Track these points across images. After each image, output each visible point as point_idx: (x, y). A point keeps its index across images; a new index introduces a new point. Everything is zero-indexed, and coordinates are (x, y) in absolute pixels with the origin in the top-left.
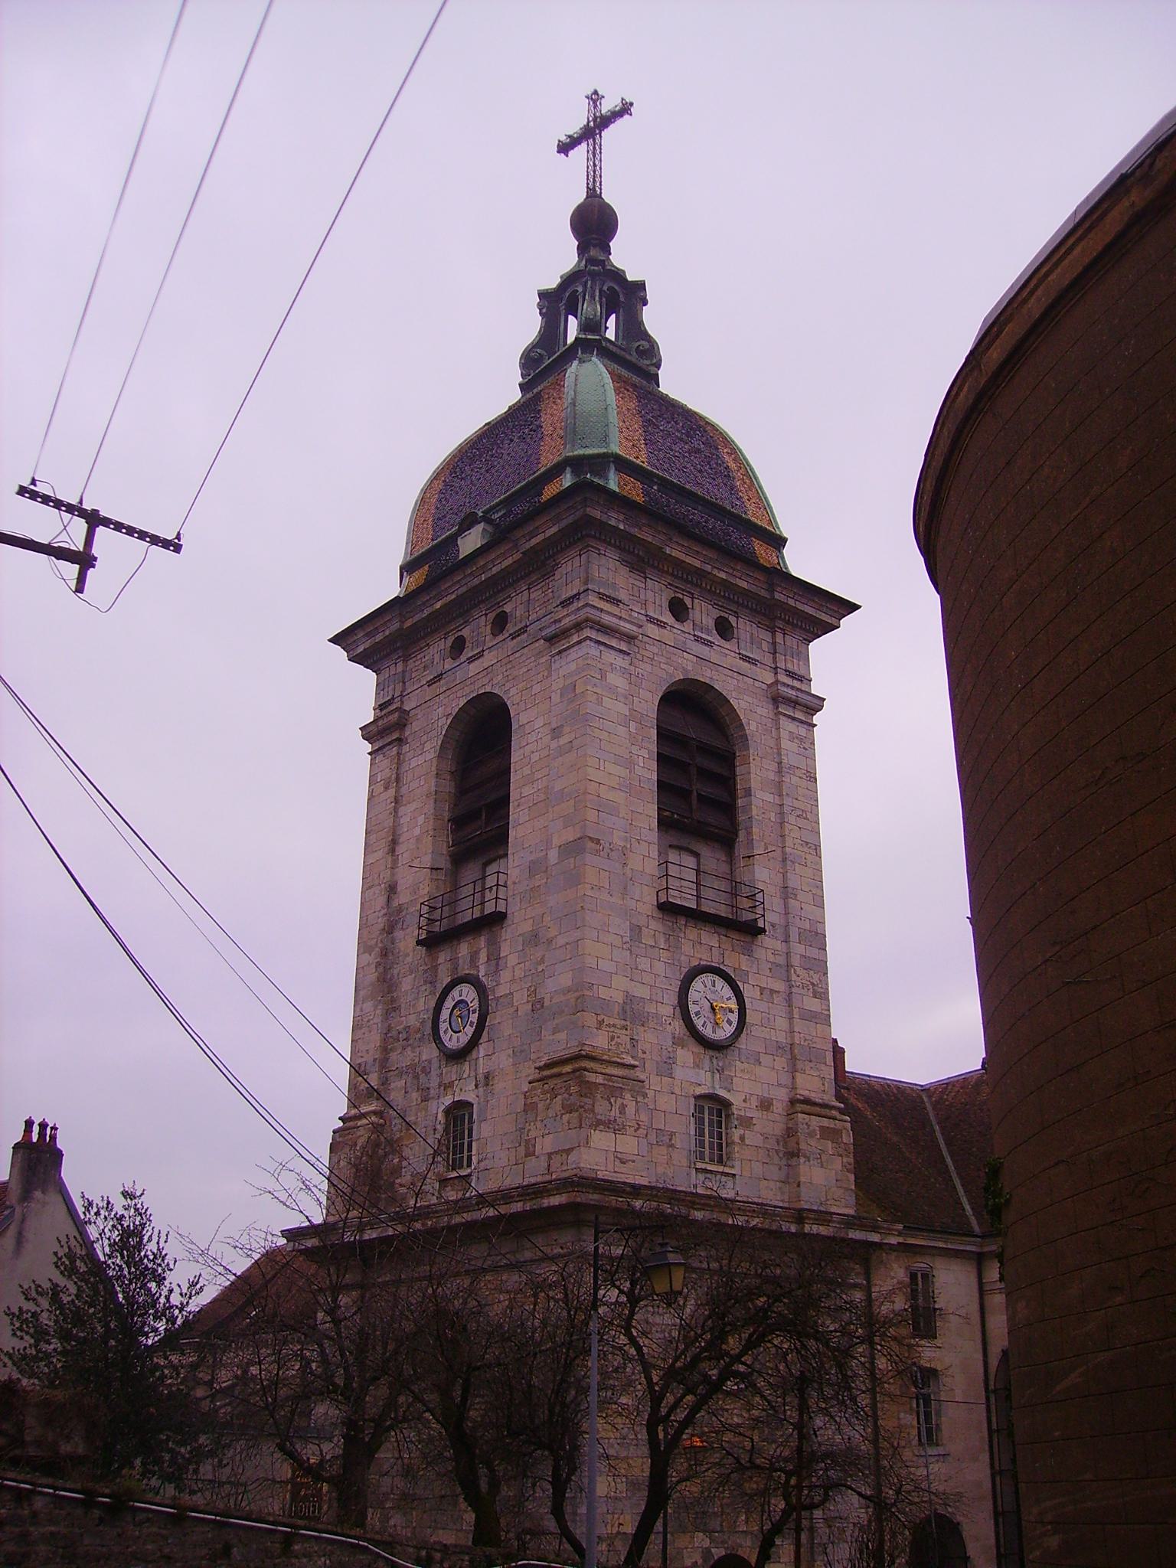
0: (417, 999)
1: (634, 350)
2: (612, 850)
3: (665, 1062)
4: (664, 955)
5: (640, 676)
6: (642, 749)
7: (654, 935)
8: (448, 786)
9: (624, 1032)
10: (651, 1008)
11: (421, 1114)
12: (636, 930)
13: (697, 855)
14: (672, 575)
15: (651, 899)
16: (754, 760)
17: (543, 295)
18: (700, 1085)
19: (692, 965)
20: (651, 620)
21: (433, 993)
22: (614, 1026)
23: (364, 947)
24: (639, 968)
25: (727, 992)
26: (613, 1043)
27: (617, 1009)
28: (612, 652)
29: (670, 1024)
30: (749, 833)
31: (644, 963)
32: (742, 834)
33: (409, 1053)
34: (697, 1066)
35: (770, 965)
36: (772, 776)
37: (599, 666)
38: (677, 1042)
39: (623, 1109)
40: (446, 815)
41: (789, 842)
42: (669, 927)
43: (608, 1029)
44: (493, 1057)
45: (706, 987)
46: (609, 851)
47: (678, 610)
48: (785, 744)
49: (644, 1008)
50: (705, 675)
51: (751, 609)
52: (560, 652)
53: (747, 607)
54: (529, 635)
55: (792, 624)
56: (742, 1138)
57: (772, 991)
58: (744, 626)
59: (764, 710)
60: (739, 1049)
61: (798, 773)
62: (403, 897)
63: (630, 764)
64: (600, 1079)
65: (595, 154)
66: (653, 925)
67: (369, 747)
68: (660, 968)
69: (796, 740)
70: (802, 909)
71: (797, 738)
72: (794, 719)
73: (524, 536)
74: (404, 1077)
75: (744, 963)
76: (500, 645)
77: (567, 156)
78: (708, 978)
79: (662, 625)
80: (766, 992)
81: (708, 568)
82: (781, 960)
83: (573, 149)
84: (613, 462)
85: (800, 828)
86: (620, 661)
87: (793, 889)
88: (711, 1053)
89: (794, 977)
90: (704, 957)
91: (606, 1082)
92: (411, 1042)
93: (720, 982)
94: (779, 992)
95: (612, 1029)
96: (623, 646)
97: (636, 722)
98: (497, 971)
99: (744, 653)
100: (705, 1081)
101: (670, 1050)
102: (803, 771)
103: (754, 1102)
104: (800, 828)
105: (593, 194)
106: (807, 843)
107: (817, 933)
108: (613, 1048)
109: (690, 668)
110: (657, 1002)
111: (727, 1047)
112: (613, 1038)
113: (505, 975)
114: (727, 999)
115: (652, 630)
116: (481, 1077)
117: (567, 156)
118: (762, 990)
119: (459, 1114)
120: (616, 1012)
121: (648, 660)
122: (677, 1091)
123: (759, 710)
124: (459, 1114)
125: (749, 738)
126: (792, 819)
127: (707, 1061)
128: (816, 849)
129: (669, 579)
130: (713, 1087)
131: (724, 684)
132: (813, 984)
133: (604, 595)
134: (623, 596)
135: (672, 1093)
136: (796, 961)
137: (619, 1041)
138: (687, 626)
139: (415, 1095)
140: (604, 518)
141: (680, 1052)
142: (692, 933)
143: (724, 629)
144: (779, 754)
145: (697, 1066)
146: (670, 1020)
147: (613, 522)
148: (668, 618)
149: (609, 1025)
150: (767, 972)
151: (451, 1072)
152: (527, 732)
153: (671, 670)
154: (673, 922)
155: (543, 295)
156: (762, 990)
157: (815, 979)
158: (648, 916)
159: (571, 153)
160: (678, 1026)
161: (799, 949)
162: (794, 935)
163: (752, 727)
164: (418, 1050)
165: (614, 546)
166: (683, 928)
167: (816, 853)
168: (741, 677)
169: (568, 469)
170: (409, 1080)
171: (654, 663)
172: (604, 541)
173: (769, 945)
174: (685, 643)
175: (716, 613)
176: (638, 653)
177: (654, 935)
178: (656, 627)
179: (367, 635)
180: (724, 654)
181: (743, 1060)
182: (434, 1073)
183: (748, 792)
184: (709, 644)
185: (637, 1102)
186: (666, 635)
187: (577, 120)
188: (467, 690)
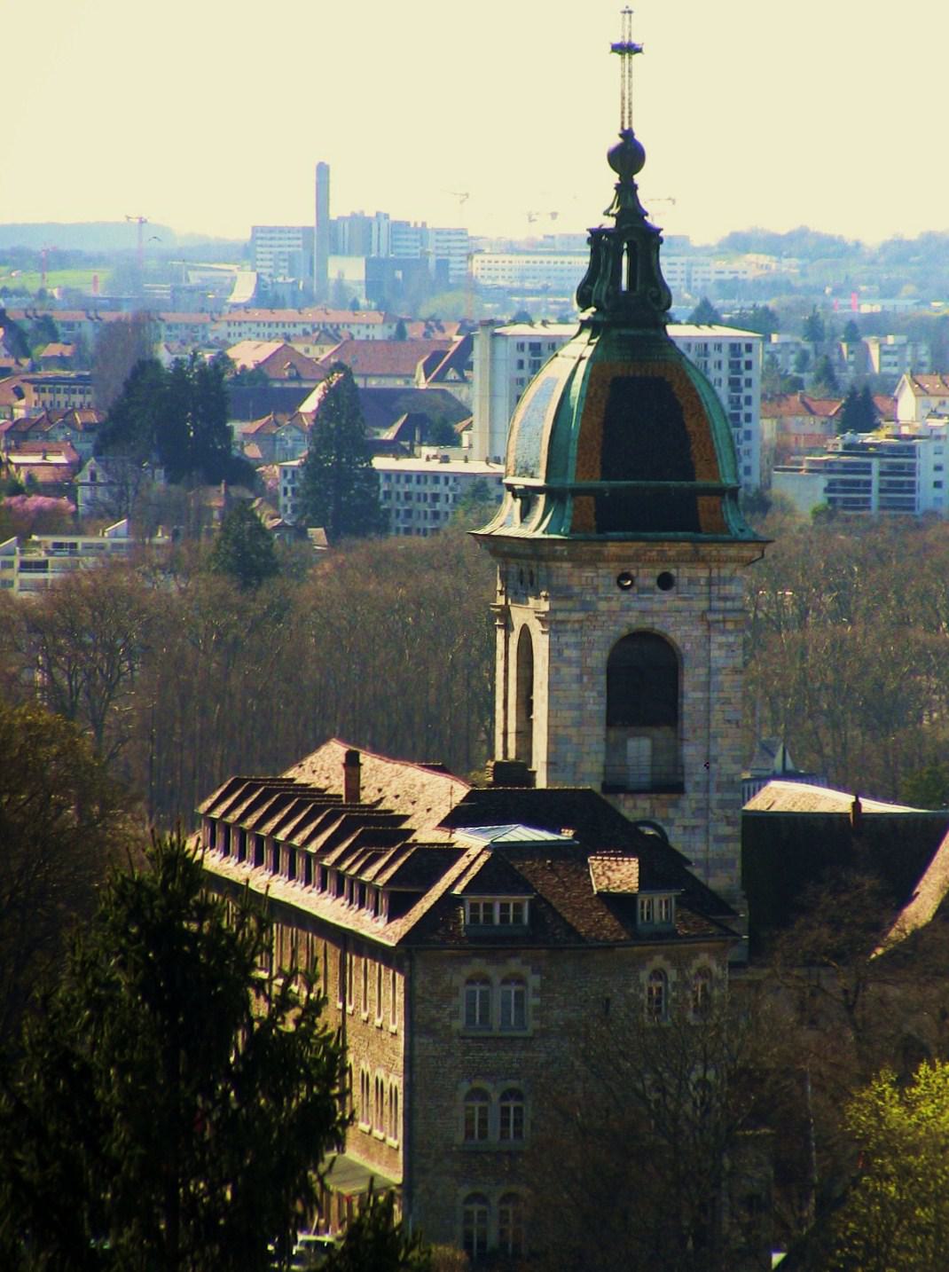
41: (713, 724)
48: (715, 653)
50: (646, 623)
61: (724, 672)
75: (671, 813)
82: (703, 805)
89: (711, 815)
105: (627, 135)
118: (685, 828)
123: (695, 633)
132: (727, 817)
136: (713, 804)
143: (666, 582)
144: (709, 661)
162: (713, 786)
173: (691, 799)
180: (668, 599)
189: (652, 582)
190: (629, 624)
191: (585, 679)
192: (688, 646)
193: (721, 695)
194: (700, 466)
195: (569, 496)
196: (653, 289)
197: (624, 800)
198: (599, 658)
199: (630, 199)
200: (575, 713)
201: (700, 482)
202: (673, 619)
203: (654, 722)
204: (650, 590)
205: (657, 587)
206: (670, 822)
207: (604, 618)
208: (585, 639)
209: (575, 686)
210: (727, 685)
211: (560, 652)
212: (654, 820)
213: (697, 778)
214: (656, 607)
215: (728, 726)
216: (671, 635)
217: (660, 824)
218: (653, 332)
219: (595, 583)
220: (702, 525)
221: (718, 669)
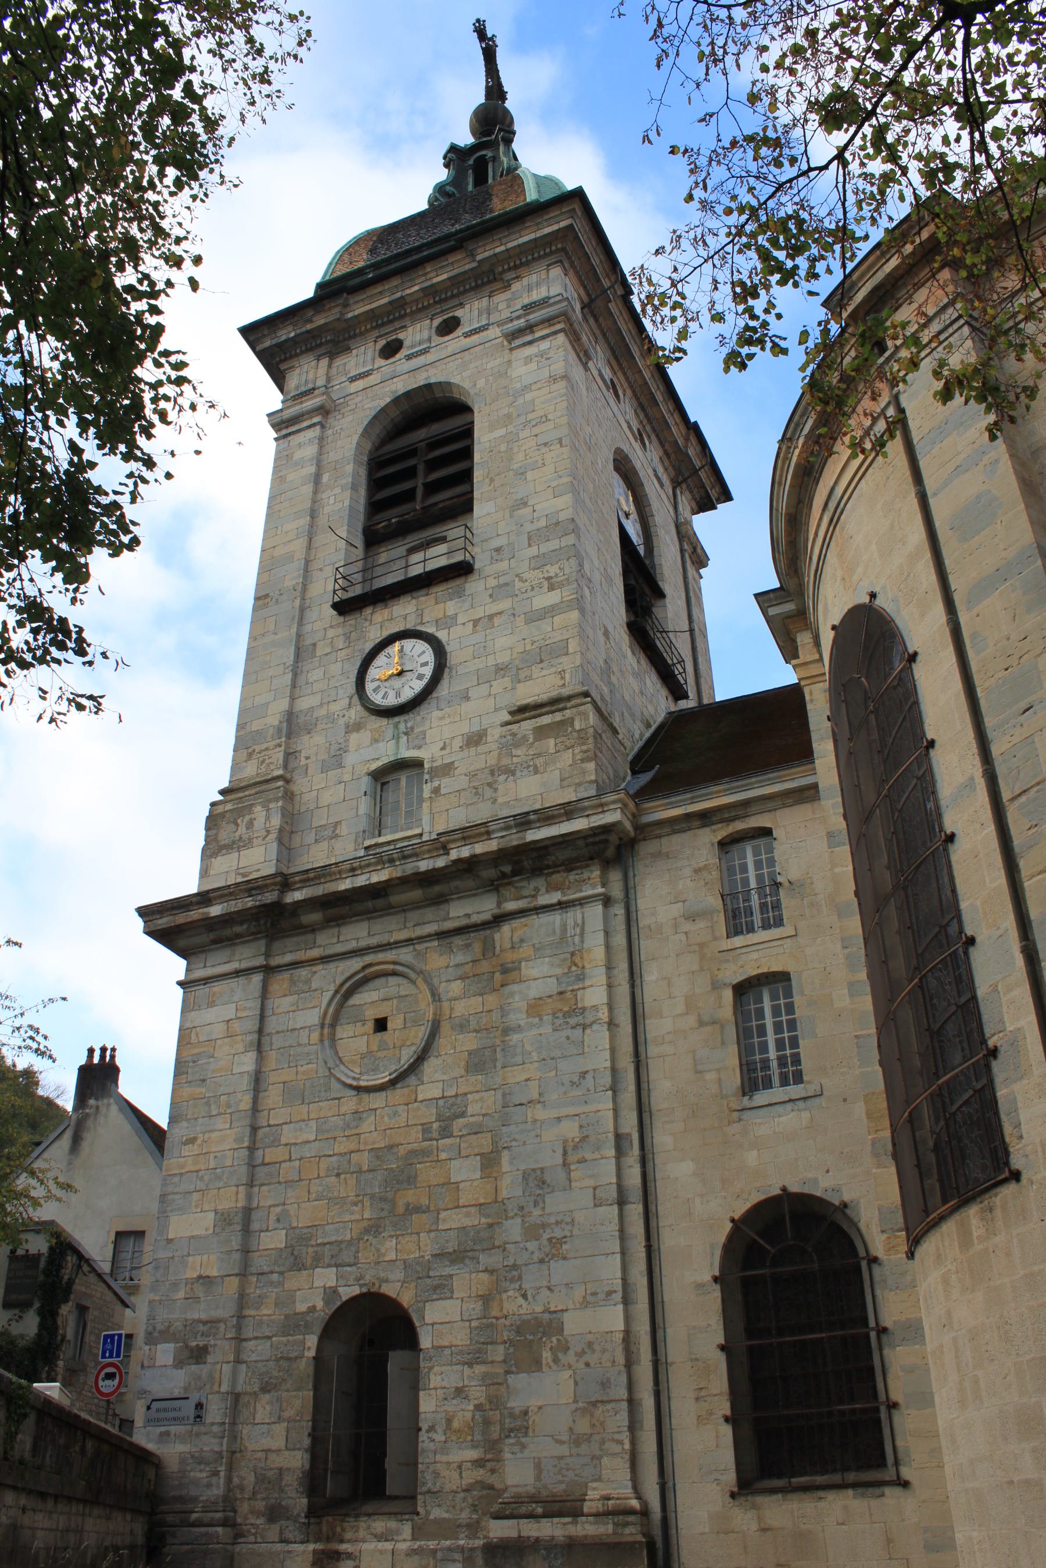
14: (373, 328)
22: (267, 749)
35: (490, 591)
39: (250, 825)
50: (420, 380)
51: (472, 289)
53: (466, 291)
55: (522, 265)
56: (436, 791)
57: (491, 617)
81: (398, 295)
88: (396, 719)
100: (386, 752)
103: (458, 743)
112: (263, 762)
118: (476, 622)
129: (376, 333)
140: (274, 342)
141: (354, 737)
143: (449, 327)
147: (284, 338)
160: (357, 712)
165: (302, 352)
172: (291, 357)
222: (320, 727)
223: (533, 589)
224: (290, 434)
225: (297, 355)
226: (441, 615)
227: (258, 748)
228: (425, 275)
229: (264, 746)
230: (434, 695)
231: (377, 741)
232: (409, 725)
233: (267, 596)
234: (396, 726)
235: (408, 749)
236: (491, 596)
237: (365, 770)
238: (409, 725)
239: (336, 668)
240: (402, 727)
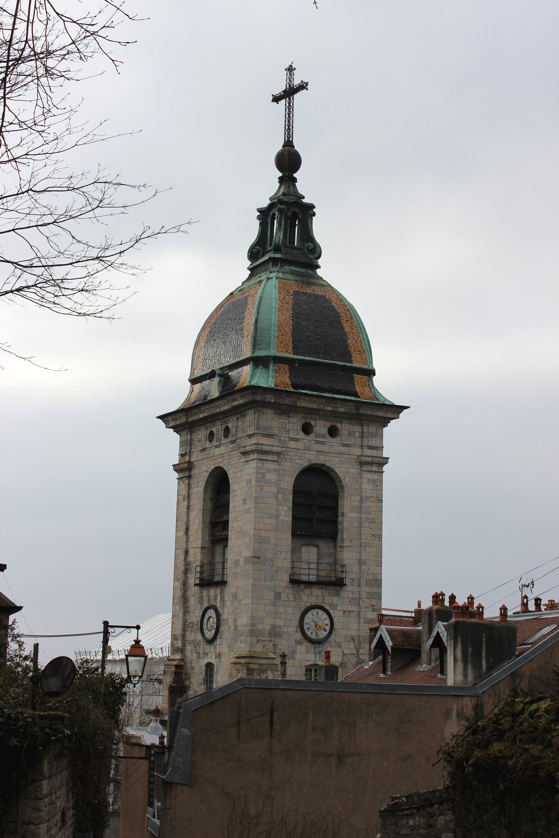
0: (196, 609)
1: (306, 248)
2: (266, 560)
3: (291, 653)
4: (292, 604)
5: (284, 470)
6: (284, 507)
7: (288, 595)
8: (209, 506)
9: (270, 643)
10: (285, 629)
11: (197, 664)
12: (278, 596)
13: (317, 547)
15: (286, 578)
16: (347, 497)
17: (260, 210)
18: (308, 661)
19: (307, 606)
20: (291, 439)
21: (201, 609)
22: (265, 641)
23: (176, 579)
24: (279, 612)
25: (325, 616)
26: (264, 649)
27: (267, 633)
28: (269, 462)
29: (294, 635)
30: (342, 535)
31: (281, 610)
32: (339, 535)
33: (193, 634)
34: (307, 652)
35: (349, 599)
36: (357, 504)
37: (262, 471)
38: (298, 643)
40: (208, 520)
41: (364, 536)
42: (295, 590)
43: (262, 643)
44: (222, 646)
45: (313, 616)
46: (265, 561)
47: (307, 429)
48: (365, 486)
49: (281, 630)
50: (321, 460)
51: (348, 418)
52: (246, 461)
54: (237, 445)
57: (350, 612)
58: (344, 428)
59: (354, 470)
60: (330, 641)
61: (371, 499)
62: (191, 558)
63: (277, 517)
64: (256, 667)
65: (290, 109)
66: (287, 590)
67: (176, 475)
68: (290, 610)
69: (372, 483)
70: (369, 569)
71: (372, 481)
72: (370, 471)
73: (231, 399)
74: (191, 645)
75: (335, 600)
76: (226, 444)
77: (278, 104)
78: (314, 612)
79: (296, 440)
80: (347, 613)
82: (356, 596)
83: (280, 100)
84: (272, 359)
85: (370, 528)
86: (273, 466)
87: (364, 560)
88: (315, 645)
89: (362, 603)
90: (313, 601)
91: (259, 667)
92: (193, 629)
93: (321, 612)
94: (353, 612)
95: (264, 642)
96: (275, 458)
97: (282, 494)
98: (223, 607)
99: (344, 442)
101: (294, 647)
102: (375, 498)
104: (370, 528)
105: (289, 143)
106: (374, 535)
107: (376, 580)
108: (265, 650)
109: (312, 458)
110: (288, 626)
111: (323, 642)
112: (264, 646)
113: (226, 610)
114: (325, 620)
115: (292, 444)
116: (217, 653)
117: (278, 104)
118: (344, 612)
119: (209, 666)
120: (266, 635)
121: (290, 460)
122: (297, 665)
123: (352, 471)
124: (209, 666)
125: (344, 487)
126: (366, 525)
127: (312, 650)
128: (379, 537)
130: (316, 661)
131: (331, 462)
132: (373, 606)
133: (265, 434)
134: (276, 431)
135: (294, 666)
136: (363, 595)
137: (267, 647)
138: (312, 435)
139: (195, 655)
141: (299, 647)
142: (307, 591)
143: (333, 432)
144: (361, 492)
145: (307, 652)
146: (294, 633)
148: (302, 435)
149: (263, 641)
150: (348, 603)
151: (207, 648)
152: (235, 495)
153: (301, 462)
154: (297, 588)
155: (260, 210)
156: (344, 612)
157: (374, 602)
158: (285, 587)
159: (279, 102)
160: (299, 636)
161: (365, 589)
162: (363, 582)
163: (346, 480)
164: (196, 634)
166: (303, 589)
167: (379, 539)
168: (342, 455)
169: (252, 363)
170: (193, 647)
171: (292, 461)
173: (350, 590)
174: (310, 446)
175: (329, 424)
176: (284, 458)
177: (288, 595)
178: (294, 442)
179: (173, 419)
180: (334, 444)
181: (332, 646)
182: (202, 647)
183: (343, 514)
184: (323, 443)
185: (274, 674)
186: (300, 445)
187: (280, 88)
188: (214, 462)
189: (325, 431)
190: (310, 460)
191: (280, 496)
192: (347, 480)
193: (369, 516)
194: (355, 356)
195: (272, 362)
196: (310, 244)
197: (304, 588)
198: (288, 483)
199: (292, 187)
200: (273, 521)
201: (355, 365)
202: (338, 459)
203: (320, 536)
204: (324, 436)
205: (328, 435)
206: (335, 607)
207: (293, 454)
208: (280, 467)
209: (273, 501)
210: (372, 509)
211: (264, 475)
212: (324, 605)
213: (353, 576)
214: (326, 448)
215: (373, 538)
216: (337, 470)
217: (328, 608)
218: (310, 272)
219: (287, 428)
220: (360, 394)
221: (367, 497)
222: (284, 637)
223: (367, 608)
224: (264, 460)
225: (268, 408)
226: (331, 603)
227: (262, 639)
228: (336, 404)
229: (264, 639)
230: (329, 640)
231: (308, 652)
232: (320, 650)
233: (259, 558)
234: (315, 648)
235: (319, 661)
236: (350, 601)
237: (304, 665)
238: (320, 650)
239: (290, 610)
240: (317, 649)
